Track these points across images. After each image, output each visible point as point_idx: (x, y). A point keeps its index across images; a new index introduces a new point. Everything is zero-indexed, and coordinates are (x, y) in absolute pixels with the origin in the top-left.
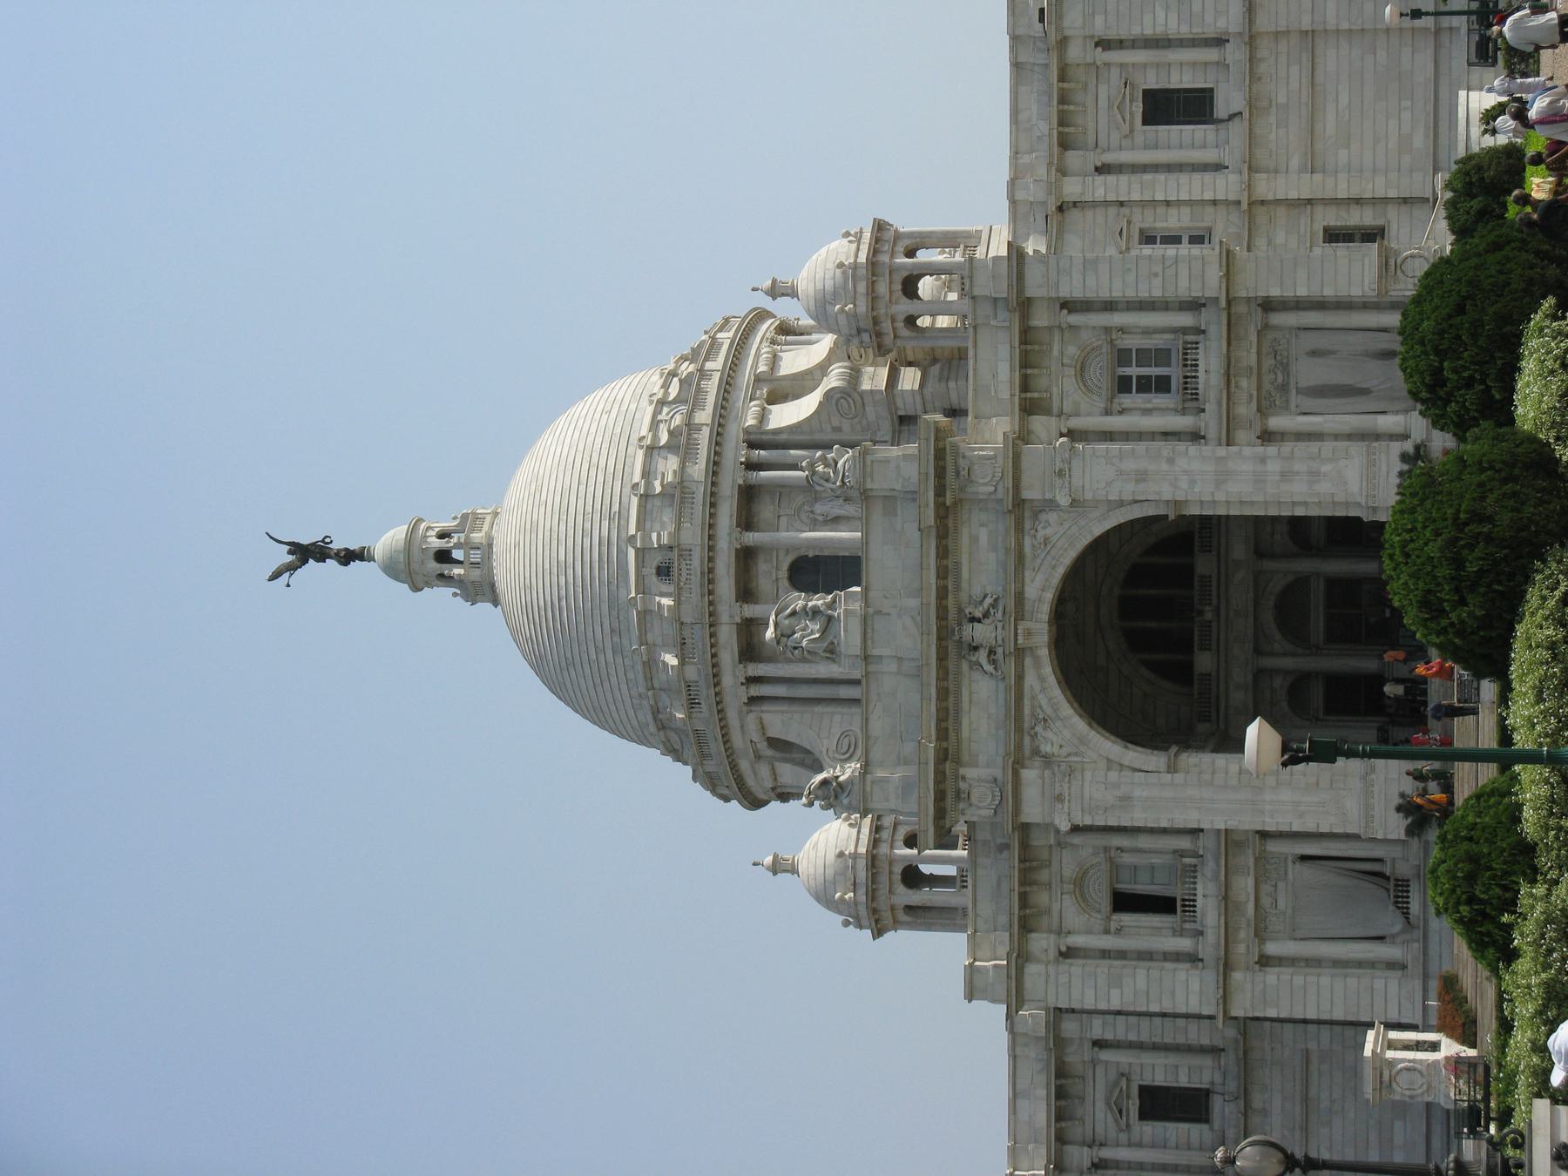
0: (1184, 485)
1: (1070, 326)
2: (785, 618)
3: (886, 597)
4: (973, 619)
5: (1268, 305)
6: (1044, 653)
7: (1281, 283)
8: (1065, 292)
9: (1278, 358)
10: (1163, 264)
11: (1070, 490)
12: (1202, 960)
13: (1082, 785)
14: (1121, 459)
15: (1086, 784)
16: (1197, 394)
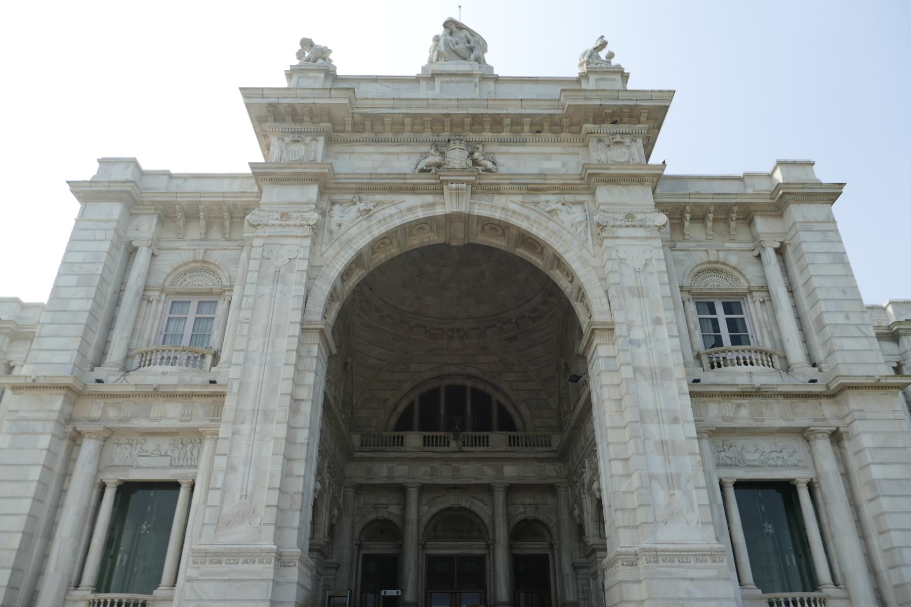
0: (638, 334)
1: (759, 256)
2: (466, 36)
3: (489, 93)
4: (471, 154)
5: (836, 437)
6: (439, 211)
7: (880, 448)
8: (804, 236)
9: (774, 455)
10: (862, 324)
11: (613, 226)
12: (92, 370)
13: (297, 237)
14: (652, 273)
15: (298, 241)
16: (719, 366)
